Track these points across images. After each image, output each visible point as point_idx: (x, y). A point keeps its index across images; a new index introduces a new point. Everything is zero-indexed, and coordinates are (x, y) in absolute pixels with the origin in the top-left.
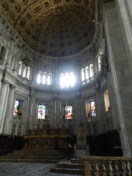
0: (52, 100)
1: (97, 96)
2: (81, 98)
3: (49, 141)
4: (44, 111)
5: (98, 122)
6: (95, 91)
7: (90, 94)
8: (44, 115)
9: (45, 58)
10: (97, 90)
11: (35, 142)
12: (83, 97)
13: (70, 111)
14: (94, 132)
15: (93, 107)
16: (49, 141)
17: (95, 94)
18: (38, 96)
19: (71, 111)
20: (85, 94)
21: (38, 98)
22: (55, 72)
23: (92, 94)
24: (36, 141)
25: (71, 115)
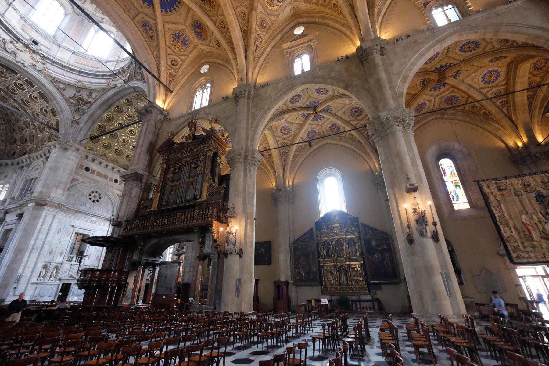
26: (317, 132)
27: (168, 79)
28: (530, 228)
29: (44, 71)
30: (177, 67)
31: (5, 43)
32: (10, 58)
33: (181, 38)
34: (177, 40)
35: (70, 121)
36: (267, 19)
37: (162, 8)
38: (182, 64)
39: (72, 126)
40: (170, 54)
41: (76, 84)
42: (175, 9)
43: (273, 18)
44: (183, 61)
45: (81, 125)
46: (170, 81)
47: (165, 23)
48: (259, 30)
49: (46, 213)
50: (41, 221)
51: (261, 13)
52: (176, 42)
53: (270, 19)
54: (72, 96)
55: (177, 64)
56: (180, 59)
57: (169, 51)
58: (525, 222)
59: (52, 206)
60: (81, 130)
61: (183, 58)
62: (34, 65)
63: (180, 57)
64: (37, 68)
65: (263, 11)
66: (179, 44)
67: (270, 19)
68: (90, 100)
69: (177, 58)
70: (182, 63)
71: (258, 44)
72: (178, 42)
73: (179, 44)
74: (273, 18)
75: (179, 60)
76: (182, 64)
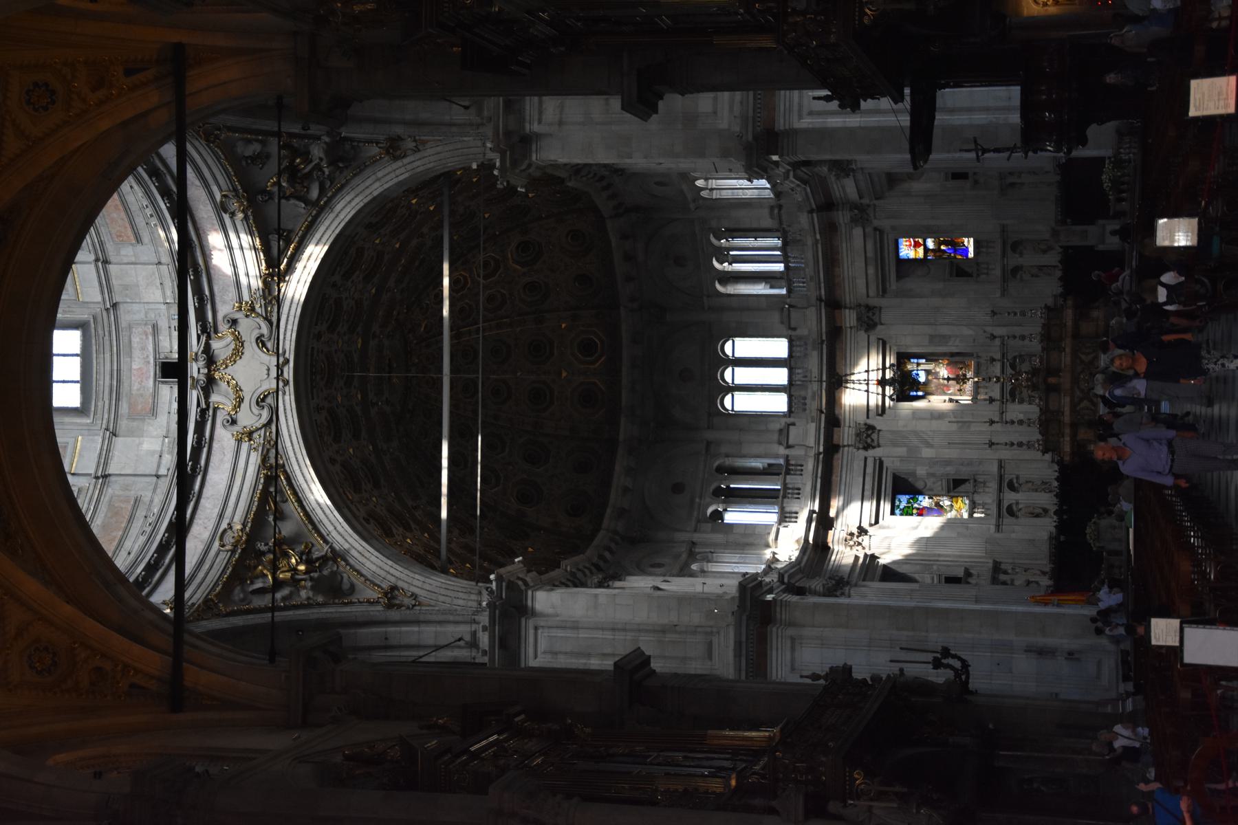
0: (871, 453)
1: (885, 224)
2: (874, 302)
3: (1083, 357)
5: (1004, 229)
6: (858, 232)
7: (870, 254)
10: (855, 221)
11: (1085, 403)
14: (1045, 252)
15: (926, 250)
16: (1083, 357)
17: (875, 229)
20: (861, 283)
22: (709, 444)
23: (870, 246)
29: (258, 309)
31: (250, 435)
32: (288, 403)
39: (417, 150)
41: (240, 215)
45: (398, 130)
46: (129, 72)
49: (800, 117)
54: (292, 201)
62: (260, 341)
64: (265, 330)
68: (273, 146)
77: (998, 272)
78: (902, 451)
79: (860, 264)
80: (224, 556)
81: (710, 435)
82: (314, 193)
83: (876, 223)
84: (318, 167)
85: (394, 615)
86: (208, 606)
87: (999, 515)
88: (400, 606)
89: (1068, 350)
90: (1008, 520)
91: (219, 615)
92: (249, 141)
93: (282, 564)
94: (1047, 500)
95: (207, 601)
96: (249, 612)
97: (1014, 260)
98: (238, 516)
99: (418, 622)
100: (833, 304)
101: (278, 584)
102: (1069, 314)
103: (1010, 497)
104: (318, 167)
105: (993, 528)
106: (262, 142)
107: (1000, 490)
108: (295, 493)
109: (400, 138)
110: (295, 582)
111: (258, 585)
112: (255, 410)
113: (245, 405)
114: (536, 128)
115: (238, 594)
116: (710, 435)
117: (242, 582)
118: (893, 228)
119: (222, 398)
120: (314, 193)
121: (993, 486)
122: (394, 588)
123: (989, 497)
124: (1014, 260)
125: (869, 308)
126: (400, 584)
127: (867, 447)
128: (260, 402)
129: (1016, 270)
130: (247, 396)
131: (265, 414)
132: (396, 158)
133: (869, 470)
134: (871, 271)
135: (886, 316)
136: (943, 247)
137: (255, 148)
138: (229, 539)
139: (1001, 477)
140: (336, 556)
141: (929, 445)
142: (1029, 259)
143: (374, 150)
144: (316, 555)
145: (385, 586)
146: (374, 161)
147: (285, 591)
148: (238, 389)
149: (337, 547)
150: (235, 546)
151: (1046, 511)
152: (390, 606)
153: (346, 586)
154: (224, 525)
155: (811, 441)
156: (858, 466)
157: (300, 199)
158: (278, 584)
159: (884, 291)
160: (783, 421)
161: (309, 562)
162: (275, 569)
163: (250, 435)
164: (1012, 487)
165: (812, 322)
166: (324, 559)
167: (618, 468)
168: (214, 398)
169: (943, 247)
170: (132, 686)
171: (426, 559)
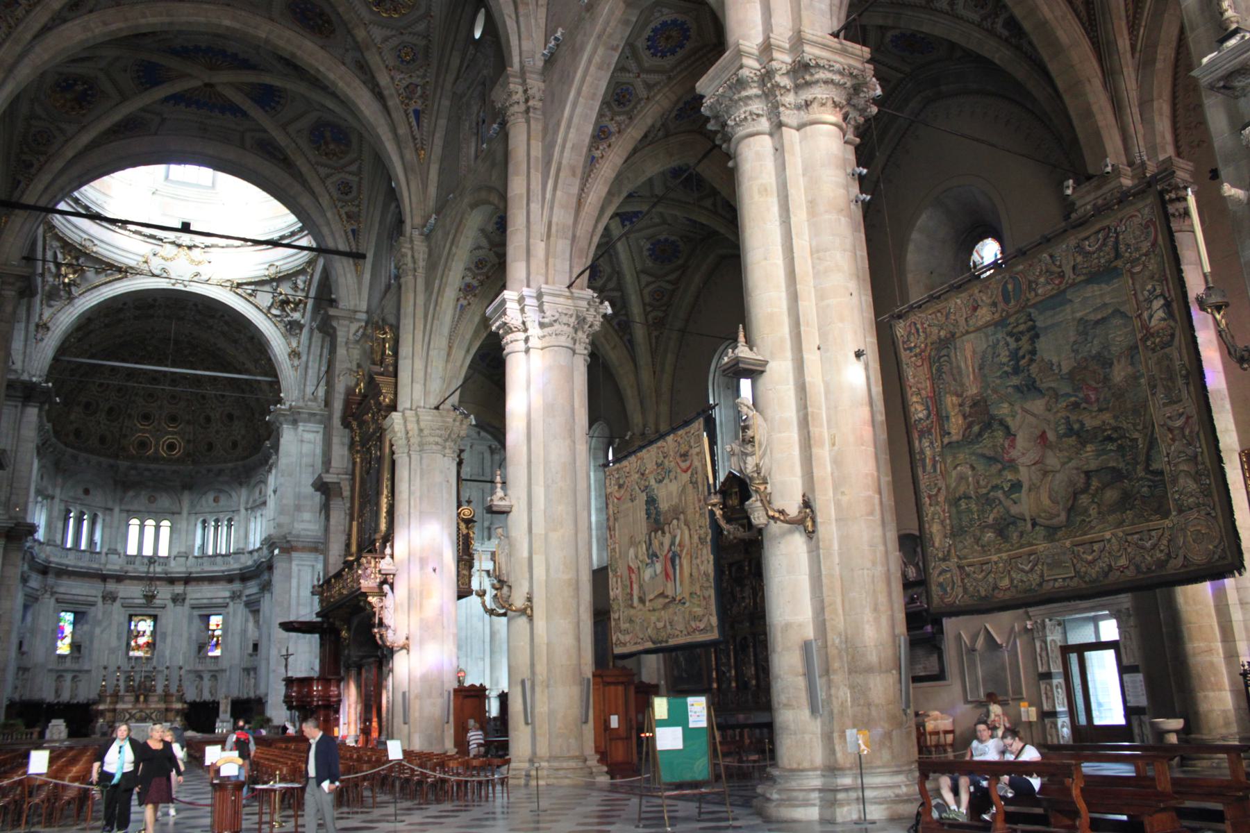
0: (100, 600)
2: (187, 602)
4: (68, 629)
5: (223, 671)
6: (227, 594)
7: (214, 601)
8: (68, 640)
9: (89, 462)
11: (127, 716)
12: (193, 602)
13: (144, 632)
14: (211, 692)
15: (214, 630)
18: (62, 590)
19: (148, 633)
20: (198, 595)
21: (62, 596)
22: (111, 510)
23: (219, 601)
24: (130, 714)
25: (151, 646)
26: (673, 238)
27: (349, 228)
28: (633, 576)
30: (354, 194)
33: (328, 134)
34: (322, 142)
35: (287, 357)
36: (407, 38)
37: (263, 108)
38: (360, 183)
39: (293, 366)
40: (328, 176)
42: (280, 97)
43: (421, 27)
44: (359, 173)
45: (304, 358)
46: (353, 231)
47: (284, 127)
48: (402, 76)
49: (298, 565)
50: (294, 582)
51: (386, 39)
52: (323, 147)
53: (415, 34)
54: (271, 300)
55: (351, 187)
56: (350, 173)
57: (323, 171)
58: (631, 564)
59: (303, 549)
60: (307, 368)
61: (354, 168)
63: (348, 169)
65: (388, 33)
66: (332, 146)
67: (415, 34)
68: (300, 295)
69: (342, 175)
70: (356, 179)
71: (419, 106)
72: (327, 143)
73: (332, 146)
74: (421, 27)
75: (350, 177)
76: (360, 183)
77: (200, 668)
78: (100, 616)
79: (209, 595)
80: (78, 239)
81: (117, 510)
82: (274, 311)
83: (231, 604)
84: (288, 315)
85: (32, 327)
86: (52, 227)
87: (57, 671)
88: (37, 331)
89: (159, 706)
90: (54, 676)
91: (45, 232)
92: (305, 282)
93: (70, 270)
94: (65, 697)
95: (54, 227)
96: (44, 249)
97: (206, 677)
98: (101, 250)
99: (26, 340)
100: (188, 580)
101: (58, 265)
102: (179, 706)
103: (69, 677)
104: (288, 315)
105: (50, 667)
106: (303, 290)
107: (73, 671)
108: (110, 282)
109: (299, 358)
110: (58, 275)
111: (60, 256)
112: (160, 267)
113: (163, 261)
114: (301, 428)
115: (56, 244)
116: (117, 510)
117: (63, 247)
118: (228, 613)
119: (169, 250)
120: (274, 311)
121: (76, 667)
122: (48, 329)
123: (68, 664)
124: (206, 677)
125: (184, 600)
126: (50, 333)
127: (104, 598)
128: (164, 270)
129: (201, 678)
130: (169, 262)
131: (157, 272)
132: (289, 355)
133: (90, 599)
134: (205, 601)
135: (179, 609)
136: (215, 639)
137: (301, 285)
138: (88, 244)
139: (80, 671)
140: (71, 299)
141: (102, 632)
142: (207, 683)
143: (294, 344)
144: (73, 289)
145: (50, 325)
146: (289, 344)
147: (53, 269)
148: (172, 259)
149: (76, 300)
150: (83, 246)
151: (59, 696)
152: (37, 326)
153: (52, 303)
154: (96, 242)
155: (109, 567)
156: (94, 592)
157: (272, 304)
158: (58, 265)
159: (193, 608)
160: (122, 552)
161: (69, 285)
162: (69, 265)
163: (146, 262)
164: (74, 677)
165: (177, 568)
166: (70, 293)
167: (102, 459)
168: (168, 246)
169: (215, 639)
170: (19, 182)
171: (62, 350)
